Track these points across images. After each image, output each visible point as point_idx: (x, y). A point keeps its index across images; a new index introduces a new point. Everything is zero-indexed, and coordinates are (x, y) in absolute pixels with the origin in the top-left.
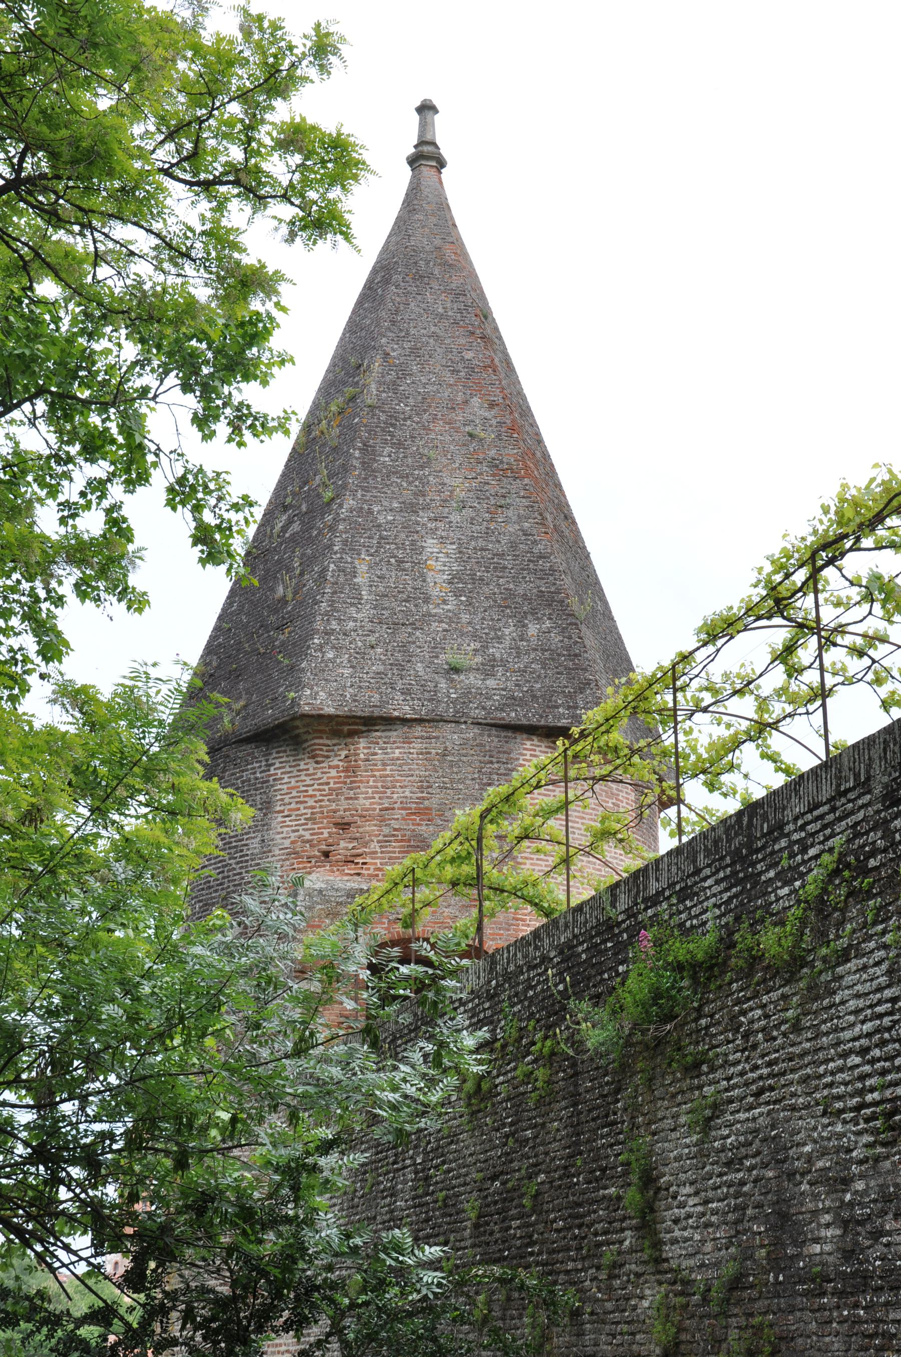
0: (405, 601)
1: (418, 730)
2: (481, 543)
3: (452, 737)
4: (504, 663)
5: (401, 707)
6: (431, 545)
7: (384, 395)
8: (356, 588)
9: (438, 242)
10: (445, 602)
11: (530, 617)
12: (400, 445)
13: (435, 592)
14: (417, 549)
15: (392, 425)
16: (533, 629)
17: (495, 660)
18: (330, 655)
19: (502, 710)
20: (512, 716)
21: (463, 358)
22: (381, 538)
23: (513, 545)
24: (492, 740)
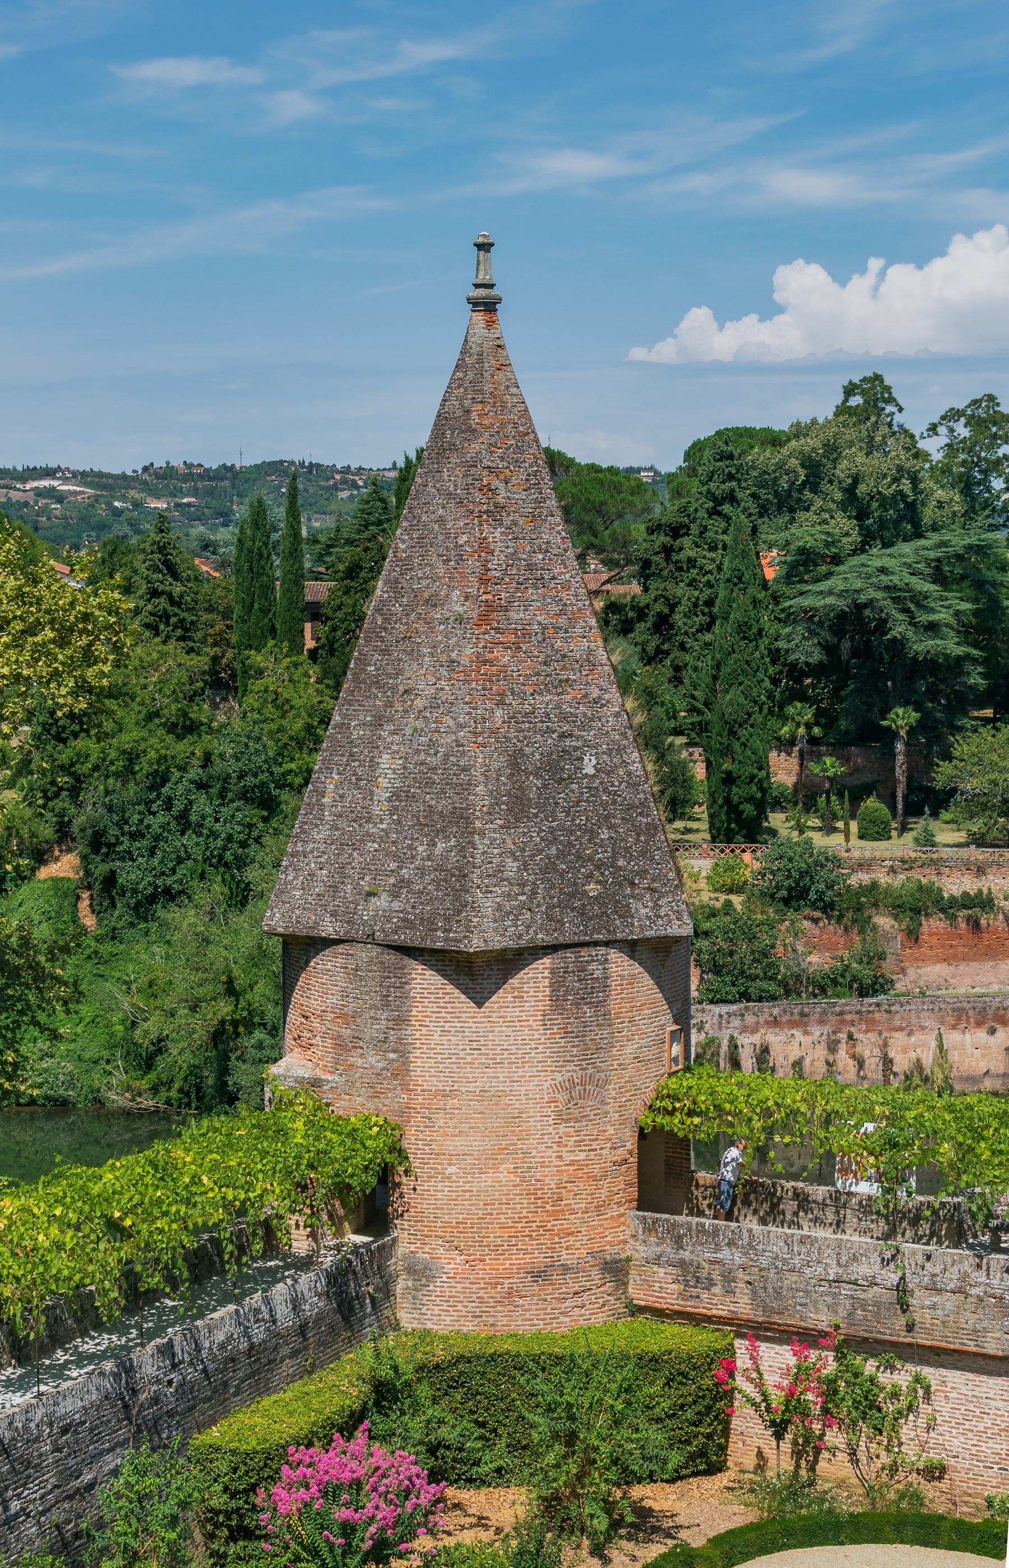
0: (354, 821)
1: (340, 948)
2: (422, 757)
3: (364, 954)
4: (410, 882)
5: (329, 929)
6: (385, 760)
7: (386, 595)
8: (322, 807)
9: (467, 403)
10: (382, 821)
11: (441, 836)
12: (385, 652)
13: (376, 810)
14: (374, 765)
15: (385, 629)
16: (440, 846)
17: (403, 881)
18: (290, 878)
19: (396, 932)
20: (402, 938)
21: (457, 546)
22: (351, 755)
23: (446, 755)
24: (391, 958)
